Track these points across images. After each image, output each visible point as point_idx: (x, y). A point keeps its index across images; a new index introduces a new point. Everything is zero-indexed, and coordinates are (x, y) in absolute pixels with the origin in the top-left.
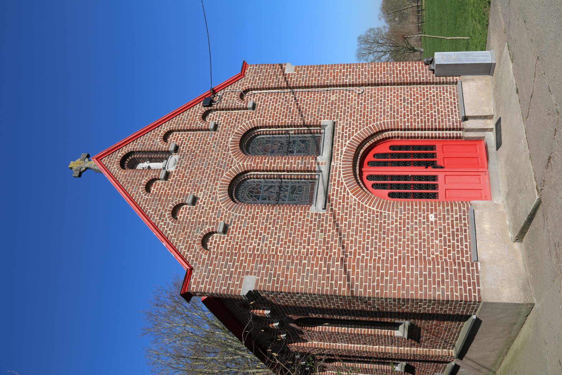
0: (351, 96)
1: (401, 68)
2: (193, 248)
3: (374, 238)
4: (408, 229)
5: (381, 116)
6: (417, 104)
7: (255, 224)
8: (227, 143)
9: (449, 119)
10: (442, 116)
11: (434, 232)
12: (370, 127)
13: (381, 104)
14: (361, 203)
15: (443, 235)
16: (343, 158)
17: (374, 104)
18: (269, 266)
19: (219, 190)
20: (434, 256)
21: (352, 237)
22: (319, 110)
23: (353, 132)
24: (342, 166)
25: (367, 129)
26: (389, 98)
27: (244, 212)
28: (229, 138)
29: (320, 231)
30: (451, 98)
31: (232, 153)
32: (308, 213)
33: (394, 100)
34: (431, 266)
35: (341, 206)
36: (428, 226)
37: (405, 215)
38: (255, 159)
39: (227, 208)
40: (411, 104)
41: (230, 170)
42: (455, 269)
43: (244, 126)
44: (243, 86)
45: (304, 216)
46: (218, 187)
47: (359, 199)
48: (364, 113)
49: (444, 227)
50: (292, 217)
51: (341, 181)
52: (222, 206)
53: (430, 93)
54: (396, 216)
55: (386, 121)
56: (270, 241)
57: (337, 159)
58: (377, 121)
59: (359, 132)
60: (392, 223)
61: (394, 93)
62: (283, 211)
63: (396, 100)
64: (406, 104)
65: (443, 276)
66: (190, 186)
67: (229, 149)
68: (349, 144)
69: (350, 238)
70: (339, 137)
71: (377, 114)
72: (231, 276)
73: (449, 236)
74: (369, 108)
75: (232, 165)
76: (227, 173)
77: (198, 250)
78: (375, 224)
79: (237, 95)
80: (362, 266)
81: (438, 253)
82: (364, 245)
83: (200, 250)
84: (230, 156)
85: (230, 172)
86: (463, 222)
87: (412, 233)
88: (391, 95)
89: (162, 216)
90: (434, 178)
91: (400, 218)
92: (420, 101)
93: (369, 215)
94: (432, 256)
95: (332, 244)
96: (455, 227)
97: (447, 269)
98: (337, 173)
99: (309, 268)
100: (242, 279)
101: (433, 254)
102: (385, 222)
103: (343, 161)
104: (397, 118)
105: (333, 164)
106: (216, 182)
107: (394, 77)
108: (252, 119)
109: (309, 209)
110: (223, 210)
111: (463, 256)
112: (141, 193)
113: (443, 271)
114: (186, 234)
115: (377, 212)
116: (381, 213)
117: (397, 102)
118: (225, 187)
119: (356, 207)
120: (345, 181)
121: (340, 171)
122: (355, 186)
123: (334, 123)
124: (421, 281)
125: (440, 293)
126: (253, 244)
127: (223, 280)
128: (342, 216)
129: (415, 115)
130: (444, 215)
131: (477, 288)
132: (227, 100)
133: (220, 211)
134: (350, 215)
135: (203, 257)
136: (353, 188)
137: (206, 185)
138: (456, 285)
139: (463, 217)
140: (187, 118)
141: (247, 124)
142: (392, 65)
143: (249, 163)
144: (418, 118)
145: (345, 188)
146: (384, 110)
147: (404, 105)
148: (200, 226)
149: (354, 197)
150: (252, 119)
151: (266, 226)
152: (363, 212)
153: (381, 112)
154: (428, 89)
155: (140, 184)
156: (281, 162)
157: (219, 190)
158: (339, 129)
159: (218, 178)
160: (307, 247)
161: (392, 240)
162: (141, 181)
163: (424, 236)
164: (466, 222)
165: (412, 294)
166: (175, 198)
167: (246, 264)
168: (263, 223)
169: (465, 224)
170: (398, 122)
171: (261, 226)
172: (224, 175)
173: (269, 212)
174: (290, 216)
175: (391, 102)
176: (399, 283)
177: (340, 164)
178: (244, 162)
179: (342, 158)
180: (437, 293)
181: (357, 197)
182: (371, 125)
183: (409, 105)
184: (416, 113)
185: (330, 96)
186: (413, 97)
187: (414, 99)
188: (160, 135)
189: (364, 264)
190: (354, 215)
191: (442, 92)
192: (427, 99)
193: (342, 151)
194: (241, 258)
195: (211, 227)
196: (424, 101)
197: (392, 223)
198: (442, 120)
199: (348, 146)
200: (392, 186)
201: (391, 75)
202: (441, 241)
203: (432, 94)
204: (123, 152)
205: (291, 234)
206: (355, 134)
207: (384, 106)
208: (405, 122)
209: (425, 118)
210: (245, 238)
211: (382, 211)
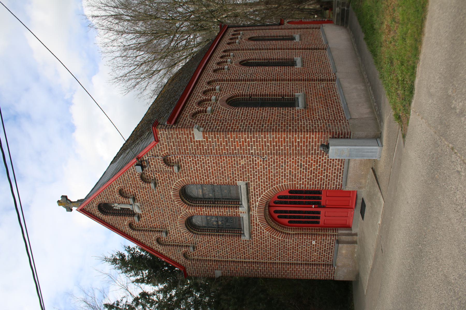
0: (257, 161)
1: (299, 140)
4: (300, 248)
5: (282, 179)
6: (310, 169)
9: (334, 183)
10: (329, 180)
12: (274, 188)
13: (282, 169)
16: (257, 210)
17: (277, 169)
19: (180, 226)
23: (262, 191)
24: (257, 215)
25: (272, 189)
26: (289, 164)
30: (338, 164)
31: (178, 203)
32: (241, 240)
33: (293, 165)
36: (311, 247)
40: (306, 169)
43: (177, 183)
48: (269, 177)
53: (323, 160)
55: (286, 183)
57: (253, 210)
58: (280, 183)
59: (266, 191)
60: (291, 245)
61: (293, 159)
63: (294, 166)
64: (302, 169)
68: (260, 200)
70: (252, 195)
71: (280, 178)
84: (177, 206)
85: (181, 216)
87: (302, 249)
88: (290, 161)
90: (319, 213)
92: (313, 167)
93: (277, 241)
98: (255, 219)
102: (286, 245)
103: (257, 212)
104: (295, 181)
105: (251, 213)
107: (293, 149)
115: (282, 240)
117: (295, 167)
122: (267, 226)
123: (246, 184)
129: (308, 179)
130: (321, 242)
142: (291, 136)
144: (311, 181)
146: (285, 174)
147: (301, 170)
149: (268, 232)
153: (282, 176)
158: (251, 189)
170: (295, 184)
175: (290, 168)
181: (269, 232)
182: (275, 187)
183: (305, 171)
184: (309, 177)
185: (240, 160)
186: (308, 163)
187: (309, 165)
192: (319, 166)
193: (256, 205)
196: (317, 167)
197: (291, 245)
198: (329, 183)
199: (259, 202)
200: (290, 217)
201: (290, 148)
202: (317, 253)
203: (324, 161)
206: (264, 193)
207: (285, 171)
208: (300, 184)
209: (316, 181)
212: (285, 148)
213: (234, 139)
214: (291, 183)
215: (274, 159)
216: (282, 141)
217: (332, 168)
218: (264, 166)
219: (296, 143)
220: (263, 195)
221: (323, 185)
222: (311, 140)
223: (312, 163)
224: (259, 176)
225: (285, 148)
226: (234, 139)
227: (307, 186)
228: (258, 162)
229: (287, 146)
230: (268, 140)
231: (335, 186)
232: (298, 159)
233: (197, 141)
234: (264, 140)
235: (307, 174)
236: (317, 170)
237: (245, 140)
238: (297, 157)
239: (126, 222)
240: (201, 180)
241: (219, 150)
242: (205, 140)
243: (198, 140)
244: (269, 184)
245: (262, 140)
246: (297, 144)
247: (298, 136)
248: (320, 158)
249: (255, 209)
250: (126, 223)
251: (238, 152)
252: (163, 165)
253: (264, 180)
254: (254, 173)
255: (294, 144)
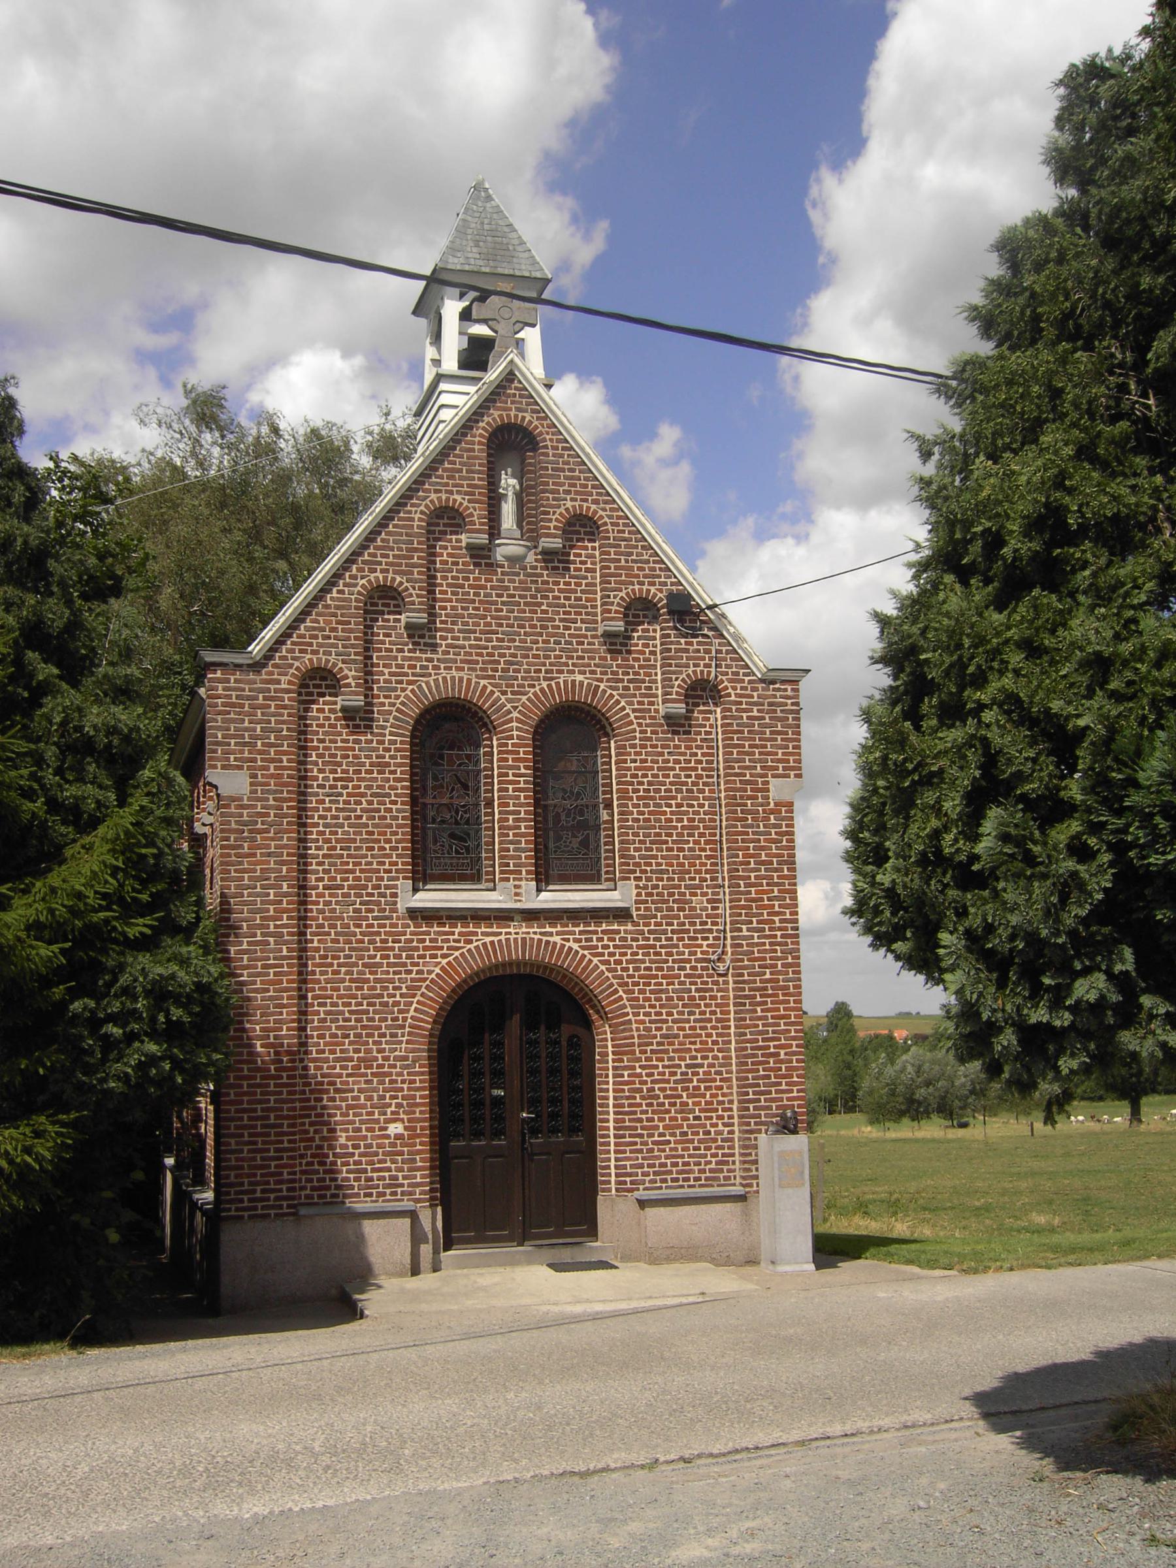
0: (705, 943)
2: (301, 651)
3: (347, 1015)
7: (367, 772)
8: (569, 672)
9: (641, 1166)
10: (652, 1150)
11: (364, 1133)
12: (616, 991)
14: (424, 985)
15: (357, 1152)
18: (272, 818)
19: (444, 678)
20: (311, 1134)
21: (347, 973)
22: (662, 872)
23: (603, 955)
24: (512, 937)
25: (612, 985)
26: (698, 1031)
27: (395, 742)
28: (580, 672)
29: (357, 906)
31: (542, 690)
32: (397, 879)
34: (285, 1129)
35: (415, 944)
37: (401, 1074)
38: (526, 746)
39: (403, 703)
41: (497, 694)
42: (281, 1174)
43: (618, 702)
44: (730, 681)
45: (390, 871)
46: (454, 672)
47: (432, 981)
48: (656, 977)
49: (377, 1154)
50: (387, 846)
51: (474, 938)
52: (408, 692)
54: (396, 1058)
56: (330, 809)
58: (632, 1007)
59: (603, 968)
61: (715, 1043)
62: (398, 826)
63: (693, 1047)
65: (268, 1150)
66: (453, 608)
67: (552, 679)
68: (570, 949)
69: (343, 969)
71: (653, 1006)
72: (245, 744)
73: (355, 1163)
74: (670, 987)
75: (510, 696)
76: (490, 688)
77: (297, 664)
78: (377, 1017)
79: (702, 672)
80: (282, 998)
81: (318, 1142)
82: (331, 997)
83: (298, 669)
84: (533, 686)
85: (492, 692)
86: (388, 1191)
88: (710, 1035)
89: (372, 565)
91: (390, 1066)
93: (396, 1004)
94: (312, 1129)
95: (329, 934)
96: (375, 1175)
97: (281, 1158)
99: (272, 897)
100: (240, 768)
101: (316, 1132)
102: (384, 1035)
103: (524, 939)
106: (466, 666)
108: (636, 718)
109: (405, 878)
110: (397, 697)
111: (313, 1189)
112: (427, 501)
113: (276, 1150)
114: (333, 630)
115: (405, 1019)
116: (403, 1027)
118: (453, 689)
119: (413, 976)
120: (477, 947)
121: (501, 933)
122: (464, 969)
124: (255, 1110)
125: (234, 1147)
126: (321, 776)
127: (236, 729)
128: (393, 949)
130: (401, 1153)
131: (246, 1214)
132: (687, 651)
133: (395, 689)
134: (395, 965)
135: (283, 678)
136: (460, 965)
137: (456, 647)
138: (249, 1176)
139: (399, 1190)
140: (634, 561)
141: (623, 708)
142: (793, 1034)
143: (515, 733)
144: (642, 1098)
145: (457, 949)
146: (666, 1021)
148: (353, 657)
149: (437, 970)
150: (636, 718)
151: (363, 795)
152: (404, 991)
154: (726, 1120)
155: (451, 493)
156: (521, 805)
157: (444, 678)
159: (475, 670)
160: (321, 884)
161: (342, 1051)
162: (459, 492)
163: (355, 1115)
164: (388, 1197)
165: (228, 1094)
166: (417, 585)
167: (272, 771)
168: (369, 787)
169: (384, 1194)
170: (633, 1052)
171: (363, 784)
172: (483, 682)
173: (396, 795)
174: (388, 841)
176: (249, 1069)
177: (517, 933)
178: (518, 720)
179: (532, 936)
180: (233, 1141)
181: (438, 975)
185: (704, 894)
187: (697, 1088)
188: (585, 505)
189: (285, 1002)
190: (395, 973)
191: (720, 1152)
193: (551, 934)
194: (285, 758)
195: (350, 680)
198: (641, 1151)
199: (563, 946)
203: (712, 1130)
204: (536, 423)
205: (349, 848)
206: (595, 960)
209: (646, 1112)
210: (334, 756)
211: (407, 1029)
212: (760, 1018)
213: (777, 884)
214: (636, 1040)
215: (712, 990)
216: (778, 1010)
217: (690, 1156)
218: (689, 961)
219: (775, 1047)
220: (589, 956)
221: (631, 1136)
222: (784, 1087)
223: (704, 1096)
224: (654, 947)
225: (760, 1018)
226: (777, 884)
227: (626, 1087)
228: (701, 946)
229: (764, 1025)
230: (779, 973)
231: (629, 1170)
232: (715, 1058)
233: (767, 783)
234: (779, 963)
235: (667, 1086)
236: (682, 1112)
237: (777, 914)
238: (720, 1055)
239: (465, 503)
240: (636, 776)
241: (743, 841)
242: (772, 805)
243: (771, 786)
244: (629, 976)
245: (778, 959)
246: (772, 1050)
247: (794, 1053)
248: (719, 1117)
249: (535, 933)
250: (458, 498)
251: (741, 893)
252: (688, 675)
253: (643, 962)
254: (665, 932)
255: (771, 1044)
